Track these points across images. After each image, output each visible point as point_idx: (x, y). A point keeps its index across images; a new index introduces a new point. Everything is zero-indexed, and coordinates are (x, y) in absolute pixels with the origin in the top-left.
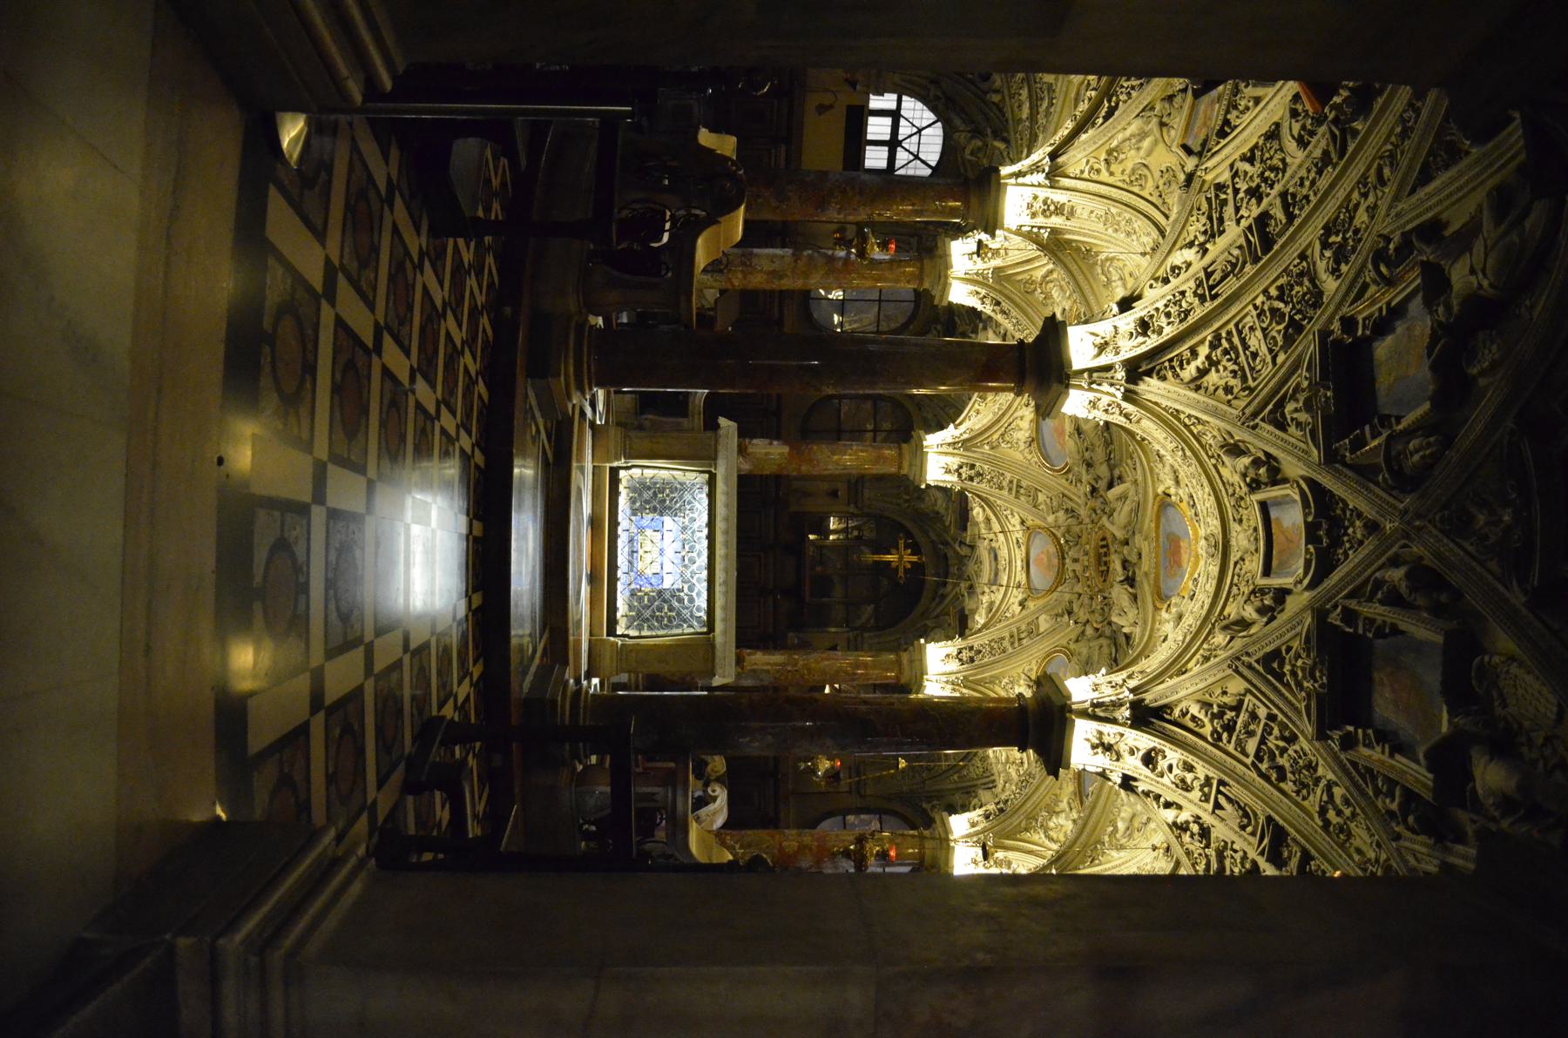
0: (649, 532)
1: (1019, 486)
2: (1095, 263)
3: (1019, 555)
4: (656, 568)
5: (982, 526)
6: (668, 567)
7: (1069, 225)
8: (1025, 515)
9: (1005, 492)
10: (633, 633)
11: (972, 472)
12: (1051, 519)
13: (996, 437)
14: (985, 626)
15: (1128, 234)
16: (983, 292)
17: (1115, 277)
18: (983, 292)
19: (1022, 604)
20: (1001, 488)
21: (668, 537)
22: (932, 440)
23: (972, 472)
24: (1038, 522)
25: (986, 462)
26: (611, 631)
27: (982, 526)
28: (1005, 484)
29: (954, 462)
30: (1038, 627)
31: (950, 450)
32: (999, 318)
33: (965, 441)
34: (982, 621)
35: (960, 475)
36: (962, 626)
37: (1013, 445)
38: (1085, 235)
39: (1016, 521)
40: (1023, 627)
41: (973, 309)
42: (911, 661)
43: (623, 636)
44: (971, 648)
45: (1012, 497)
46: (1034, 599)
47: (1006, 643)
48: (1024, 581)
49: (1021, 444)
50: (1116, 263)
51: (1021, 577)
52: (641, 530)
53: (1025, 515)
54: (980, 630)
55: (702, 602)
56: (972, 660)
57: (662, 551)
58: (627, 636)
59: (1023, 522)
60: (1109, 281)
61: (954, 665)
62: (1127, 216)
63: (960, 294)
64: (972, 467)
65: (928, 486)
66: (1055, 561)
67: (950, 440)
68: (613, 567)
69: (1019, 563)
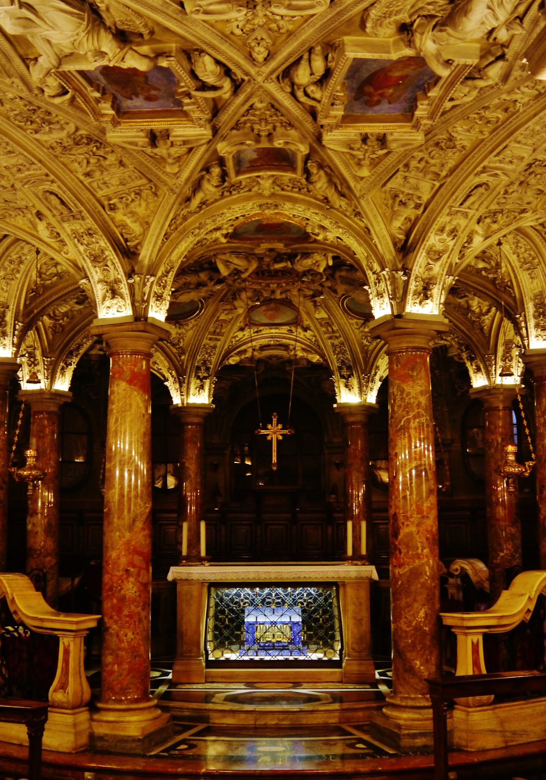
0: (258, 635)
1: (214, 333)
2: (43, 286)
3: (266, 331)
4: (287, 629)
5: (243, 357)
6: (286, 619)
7: (12, 307)
8: (236, 328)
9: (219, 344)
10: (338, 647)
11: (203, 368)
12: (240, 311)
13: (174, 350)
14: (322, 356)
15: (21, 262)
16: (62, 364)
17: (53, 270)
18: (62, 364)
19: (305, 329)
20: (215, 347)
21: (261, 619)
22: (177, 400)
23: (203, 368)
24: (241, 319)
25: (194, 358)
26: (337, 664)
27: (243, 357)
28: (212, 344)
29: (194, 383)
30: (322, 319)
31: (185, 385)
32: (82, 351)
33: (179, 374)
34: (318, 357)
35: (205, 378)
36: (322, 372)
37: (181, 337)
38: (21, 294)
39: (240, 334)
40: (324, 329)
41: (75, 371)
42: (351, 414)
43: (341, 655)
44: (340, 368)
45: (222, 339)
46: (302, 321)
47: (336, 342)
48: (288, 328)
49: (180, 331)
50: (43, 270)
51: (284, 330)
52: (255, 641)
53: (236, 328)
54: (326, 361)
55: (312, 590)
56: (349, 368)
57: (274, 623)
58: (341, 650)
59: (242, 329)
60: (57, 274)
61: (354, 381)
62: (7, 263)
63: (63, 384)
64: (198, 368)
65: (213, 402)
66: (272, 305)
67: (177, 386)
68: (286, 664)
69: (273, 331)
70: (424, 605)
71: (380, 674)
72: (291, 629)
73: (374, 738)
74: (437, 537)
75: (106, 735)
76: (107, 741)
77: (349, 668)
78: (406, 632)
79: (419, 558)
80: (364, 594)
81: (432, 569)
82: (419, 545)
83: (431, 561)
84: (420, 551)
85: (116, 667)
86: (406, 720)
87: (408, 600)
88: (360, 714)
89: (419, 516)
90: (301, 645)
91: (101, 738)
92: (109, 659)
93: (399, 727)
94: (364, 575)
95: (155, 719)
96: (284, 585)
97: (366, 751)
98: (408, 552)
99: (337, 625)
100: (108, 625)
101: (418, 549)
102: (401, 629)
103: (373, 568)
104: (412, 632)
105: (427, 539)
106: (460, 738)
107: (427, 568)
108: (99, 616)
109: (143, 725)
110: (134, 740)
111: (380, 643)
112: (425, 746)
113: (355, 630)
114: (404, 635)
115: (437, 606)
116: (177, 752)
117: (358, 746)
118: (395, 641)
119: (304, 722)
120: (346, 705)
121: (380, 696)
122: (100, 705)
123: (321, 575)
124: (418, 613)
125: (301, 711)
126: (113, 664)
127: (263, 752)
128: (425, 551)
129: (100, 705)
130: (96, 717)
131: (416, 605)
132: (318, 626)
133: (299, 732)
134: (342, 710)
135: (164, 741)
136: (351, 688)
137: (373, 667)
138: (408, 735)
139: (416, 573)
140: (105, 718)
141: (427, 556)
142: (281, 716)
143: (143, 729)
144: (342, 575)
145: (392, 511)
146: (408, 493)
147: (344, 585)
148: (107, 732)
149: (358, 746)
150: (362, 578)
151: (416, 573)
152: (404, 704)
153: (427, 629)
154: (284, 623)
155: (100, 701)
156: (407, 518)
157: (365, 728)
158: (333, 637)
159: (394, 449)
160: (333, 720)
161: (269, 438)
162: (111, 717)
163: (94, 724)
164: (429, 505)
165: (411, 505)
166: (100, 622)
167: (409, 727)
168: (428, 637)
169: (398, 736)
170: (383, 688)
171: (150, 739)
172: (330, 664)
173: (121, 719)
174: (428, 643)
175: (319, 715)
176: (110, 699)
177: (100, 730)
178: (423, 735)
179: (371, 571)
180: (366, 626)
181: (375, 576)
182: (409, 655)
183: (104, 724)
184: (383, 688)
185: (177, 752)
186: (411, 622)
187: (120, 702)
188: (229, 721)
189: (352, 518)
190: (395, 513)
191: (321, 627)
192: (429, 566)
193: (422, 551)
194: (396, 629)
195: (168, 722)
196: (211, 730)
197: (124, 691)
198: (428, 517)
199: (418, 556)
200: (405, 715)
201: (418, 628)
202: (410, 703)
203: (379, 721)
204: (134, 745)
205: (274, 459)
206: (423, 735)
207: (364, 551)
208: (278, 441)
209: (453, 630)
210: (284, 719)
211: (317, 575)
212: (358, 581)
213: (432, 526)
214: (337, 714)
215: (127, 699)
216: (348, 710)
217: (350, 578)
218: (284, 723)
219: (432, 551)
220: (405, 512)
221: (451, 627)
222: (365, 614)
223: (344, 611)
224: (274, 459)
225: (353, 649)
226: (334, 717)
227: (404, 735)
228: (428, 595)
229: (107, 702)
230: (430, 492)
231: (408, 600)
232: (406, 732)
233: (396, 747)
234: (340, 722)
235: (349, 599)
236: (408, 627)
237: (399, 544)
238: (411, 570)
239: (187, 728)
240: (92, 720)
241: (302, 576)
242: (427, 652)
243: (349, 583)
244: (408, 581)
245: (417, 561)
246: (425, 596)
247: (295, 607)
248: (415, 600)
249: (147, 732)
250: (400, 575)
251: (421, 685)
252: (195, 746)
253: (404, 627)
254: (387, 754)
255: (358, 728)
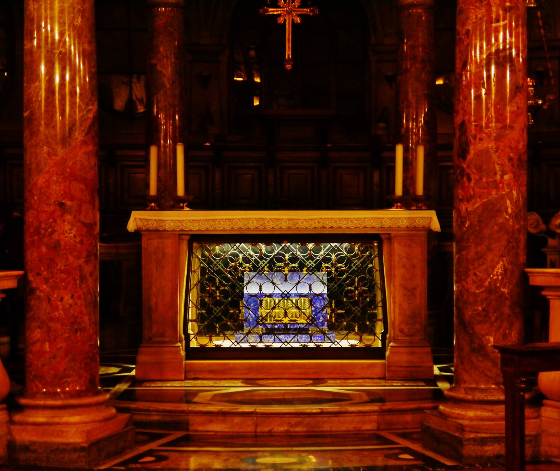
26: (379, 353)
43: (383, 340)
58: (384, 335)
70: (502, 256)
71: (441, 369)
72: (311, 303)
73: (425, 447)
74: (525, 158)
75: (33, 443)
76: (35, 451)
77: (396, 358)
78: (474, 294)
79: (497, 188)
80: (419, 254)
81: (515, 204)
82: (497, 167)
83: (514, 192)
84: (498, 177)
85: (47, 346)
86: (471, 419)
87: (479, 249)
88: (408, 418)
89: (499, 125)
90: (325, 328)
91: (26, 448)
92: (37, 334)
93: (461, 429)
94: (420, 223)
95: (106, 420)
96: (301, 238)
97: (414, 463)
98: (481, 179)
99: (379, 298)
100: (34, 285)
101: (496, 174)
102: (467, 291)
103: (432, 215)
104: (484, 296)
105: (510, 159)
106: (550, 446)
107: (508, 202)
108: (21, 272)
109: (88, 427)
110: (75, 448)
111: (440, 323)
112: (498, 456)
113: (405, 305)
114: (471, 299)
115: (522, 258)
116: (138, 466)
117: (402, 456)
118: (459, 309)
119: (327, 428)
120: (388, 406)
121: (439, 396)
122: (23, 401)
123: (356, 224)
124: (494, 268)
125: (322, 413)
126: (43, 342)
127: (265, 464)
128: (506, 177)
129: (23, 401)
130: (17, 417)
131: (490, 257)
132: (350, 303)
133: (319, 440)
134: (381, 412)
135: (120, 452)
136: (397, 386)
137: (430, 358)
138: (474, 440)
139: (492, 210)
140: (31, 420)
141: (509, 185)
142: (294, 420)
143: (88, 433)
144: (387, 224)
145: (458, 120)
146: (483, 91)
147: (390, 238)
148: (34, 439)
149: (402, 456)
150: (415, 228)
151: (492, 210)
152: (469, 397)
153: (505, 290)
154: (301, 296)
155: (23, 394)
156: (479, 128)
157: (415, 436)
158: (373, 318)
159: (464, 24)
160: (369, 427)
161: (281, 20)
162: (41, 418)
163: (14, 428)
164: (515, 108)
165: (488, 109)
166: (23, 281)
167: (476, 430)
168: (508, 303)
169: (460, 441)
170: (443, 386)
171: (98, 448)
172: (368, 352)
173: (56, 420)
174: (507, 310)
175: (349, 419)
176: (39, 391)
177: (23, 436)
178: (495, 440)
179: (430, 219)
180: (421, 299)
181: (436, 226)
182: (478, 328)
183: (29, 428)
184: (443, 386)
185: (138, 466)
186: (482, 281)
187: (54, 395)
188: (217, 427)
189: (404, 140)
190: (463, 123)
191: (356, 303)
192: (511, 200)
193: (502, 177)
194: (460, 292)
195: (127, 425)
196: (187, 440)
197: (59, 380)
198: (512, 127)
199: (496, 185)
200: (471, 414)
201: (492, 290)
202: (479, 396)
203: (434, 423)
204: (75, 456)
205: (289, 53)
206: (495, 440)
207: (420, 190)
208: (294, 24)
209: (544, 293)
210: (296, 425)
211: (350, 225)
212: (412, 232)
213: (518, 142)
214: (375, 417)
215: (63, 392)
216: (390, 411)
217: (399, 229)
218: (298, 429)
219: (516, 178)
220: (479, 119)
221: (542, 288)
222: (420, 282)
223: (389, 276)
224: (289, 53)
225: (401, 331)
226: (370, 422)
227: (469, 440)
228: (509, 242)
229: (33, 396)
230: (517, 88)
231: (479, 249)
232: (472, 436)
233: (458, 456)
234: (379, 429)
235: (396, 258)
236: (478, 288)
237: (468, 167)
238: (485, 207)
239: (154, 437)
240: (11, 422)
241: (328, 224)
242: (505, 324)
243: (396, 236)
244: (480, 221)
245: (494, 193)
246: (504, 243)
247: (318, 274)
248: (489, 249)
249: (94, 438)
250: (469, 213)
251: (495, 370)
252: (165, 458)
253: (473, 289)
254: (444, 465)
255: (404, 436)
